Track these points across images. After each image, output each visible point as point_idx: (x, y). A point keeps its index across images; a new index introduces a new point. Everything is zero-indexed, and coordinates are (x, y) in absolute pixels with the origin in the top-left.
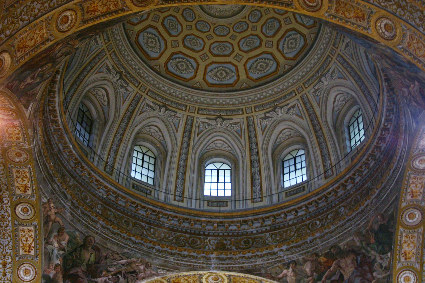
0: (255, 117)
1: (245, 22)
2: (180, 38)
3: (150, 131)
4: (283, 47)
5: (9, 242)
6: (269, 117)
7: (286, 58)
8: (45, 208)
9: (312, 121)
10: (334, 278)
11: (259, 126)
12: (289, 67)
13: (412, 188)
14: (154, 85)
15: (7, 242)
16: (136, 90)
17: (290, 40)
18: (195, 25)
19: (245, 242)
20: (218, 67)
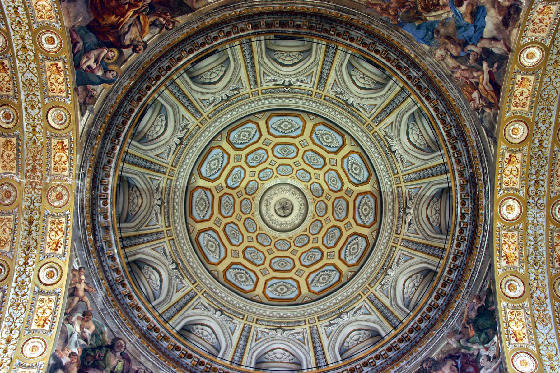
0: (319, 326)
1: (306, 235)
2: (240, 249)
3: (202, 333)
4: (345, 255)
5: (22, 315)
6: (334, 324)
7: (348, 266)
8: (74, 275)
9: (381, 312)
11: (324, 332)
12: (353, 273)
13: (506, 250)
14: (210, 289)
15: (20, 314)
16: (192, 287)
17: (352, 245)
18: (257, 237)
20: (278, 283)
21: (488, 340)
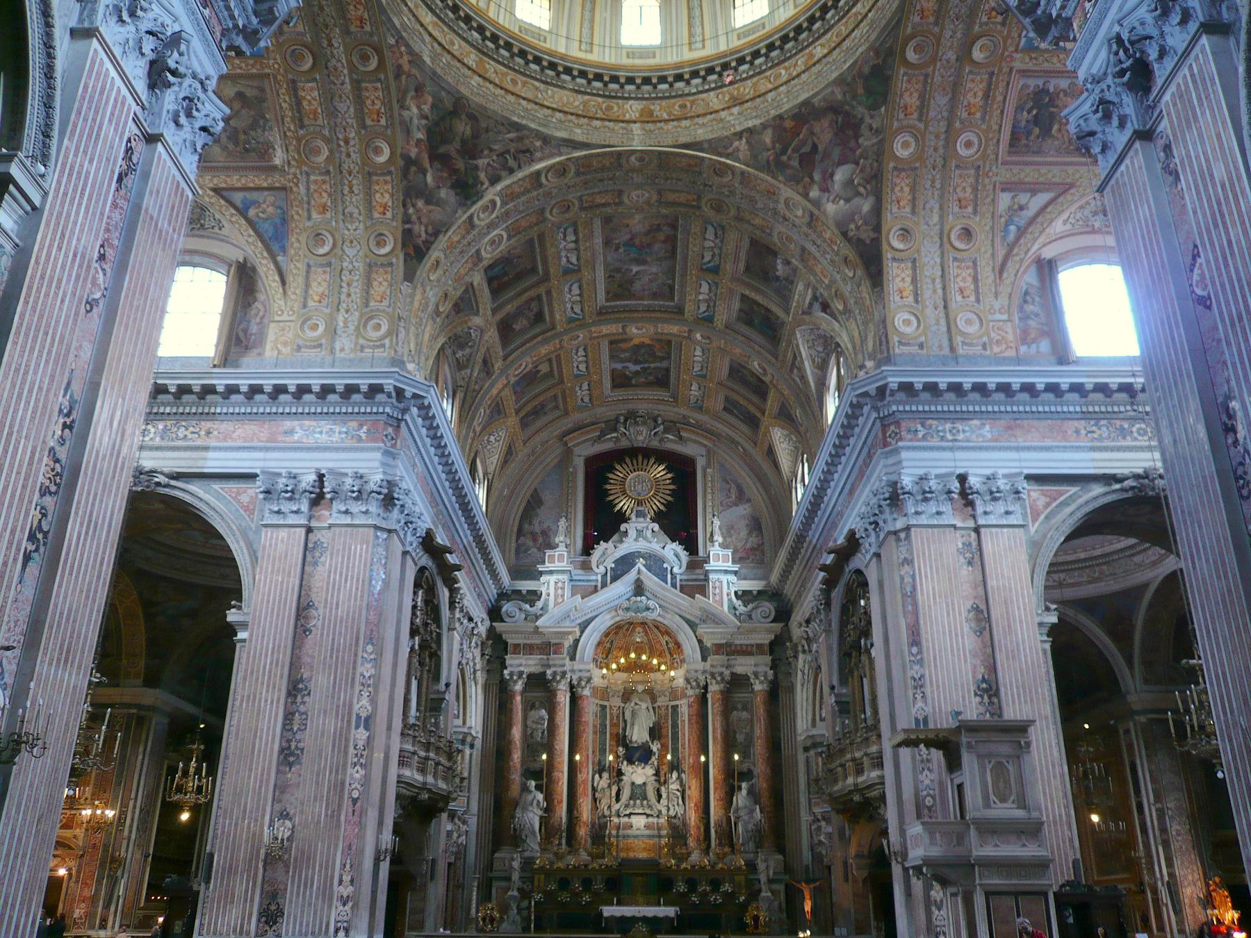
8: (393, 53)
10: (803, 150)
19: (680, 106)
21: (874, 107)
